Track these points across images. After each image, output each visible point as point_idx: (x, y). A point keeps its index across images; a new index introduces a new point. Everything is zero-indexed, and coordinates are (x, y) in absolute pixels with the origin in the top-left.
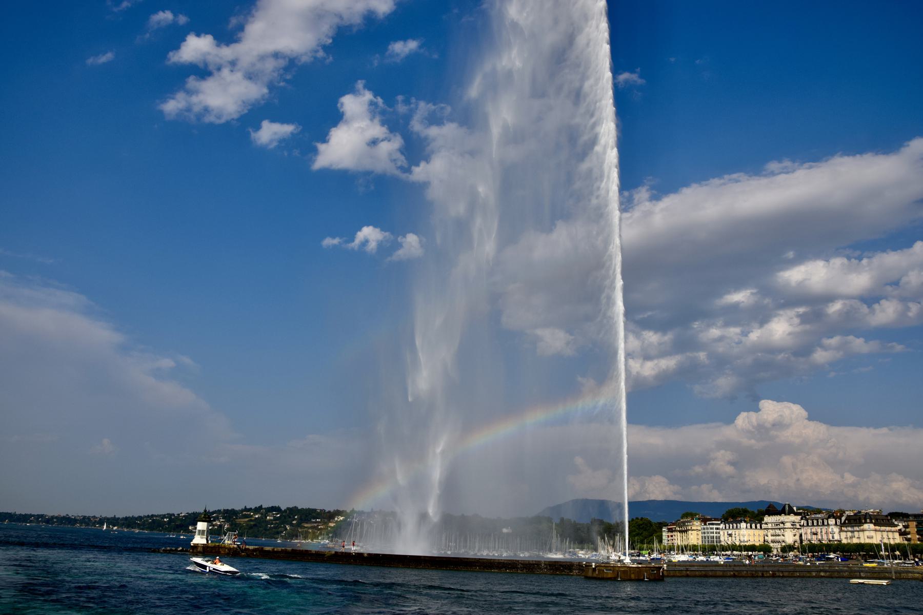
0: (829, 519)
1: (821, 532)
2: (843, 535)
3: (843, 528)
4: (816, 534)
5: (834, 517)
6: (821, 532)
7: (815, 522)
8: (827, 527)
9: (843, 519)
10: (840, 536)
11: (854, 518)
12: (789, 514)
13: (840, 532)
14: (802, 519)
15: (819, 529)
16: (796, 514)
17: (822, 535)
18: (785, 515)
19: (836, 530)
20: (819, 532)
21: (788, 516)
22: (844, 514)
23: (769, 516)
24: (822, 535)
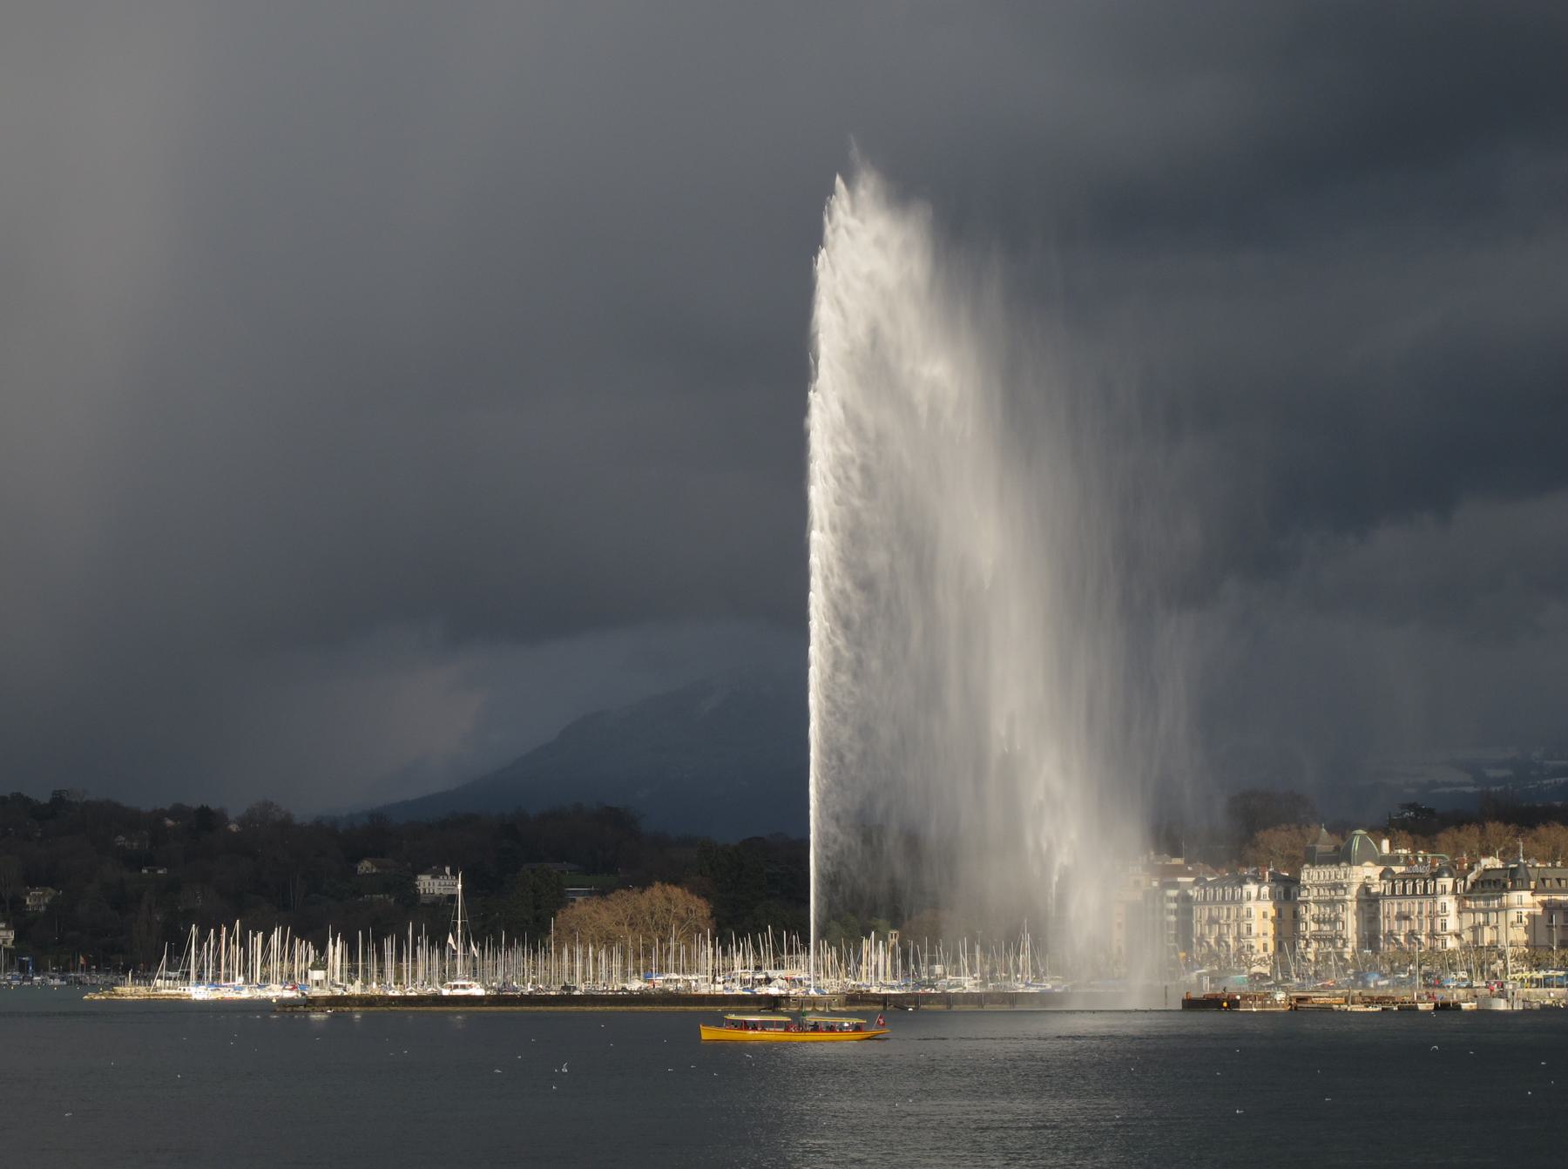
0: (1439, 880)
1: (1420, 913)
2: (1468, 919)
3: (1468, 902)
4: (1407, 918)
5: (1451, 876)
6: (1420, 913)
7: (1410, 885)
8: (1431, 900)
9: (1472, 877)
10: (1461, 924)
11: (1492, 877)
12: (1360, 864)
13: (1460, 912)
14: (1382, 876)
15: (1417, 905)
16: (1381, 861)
17: (1421, 922)
18: (1350, 863)
19: (1451, 904)
20: (1416, 913)
21: (1355, 868)
22: (1476, 866)
23: (1313, 865)
24: (1421, 922)
